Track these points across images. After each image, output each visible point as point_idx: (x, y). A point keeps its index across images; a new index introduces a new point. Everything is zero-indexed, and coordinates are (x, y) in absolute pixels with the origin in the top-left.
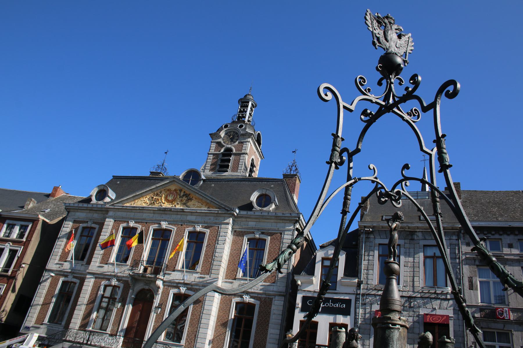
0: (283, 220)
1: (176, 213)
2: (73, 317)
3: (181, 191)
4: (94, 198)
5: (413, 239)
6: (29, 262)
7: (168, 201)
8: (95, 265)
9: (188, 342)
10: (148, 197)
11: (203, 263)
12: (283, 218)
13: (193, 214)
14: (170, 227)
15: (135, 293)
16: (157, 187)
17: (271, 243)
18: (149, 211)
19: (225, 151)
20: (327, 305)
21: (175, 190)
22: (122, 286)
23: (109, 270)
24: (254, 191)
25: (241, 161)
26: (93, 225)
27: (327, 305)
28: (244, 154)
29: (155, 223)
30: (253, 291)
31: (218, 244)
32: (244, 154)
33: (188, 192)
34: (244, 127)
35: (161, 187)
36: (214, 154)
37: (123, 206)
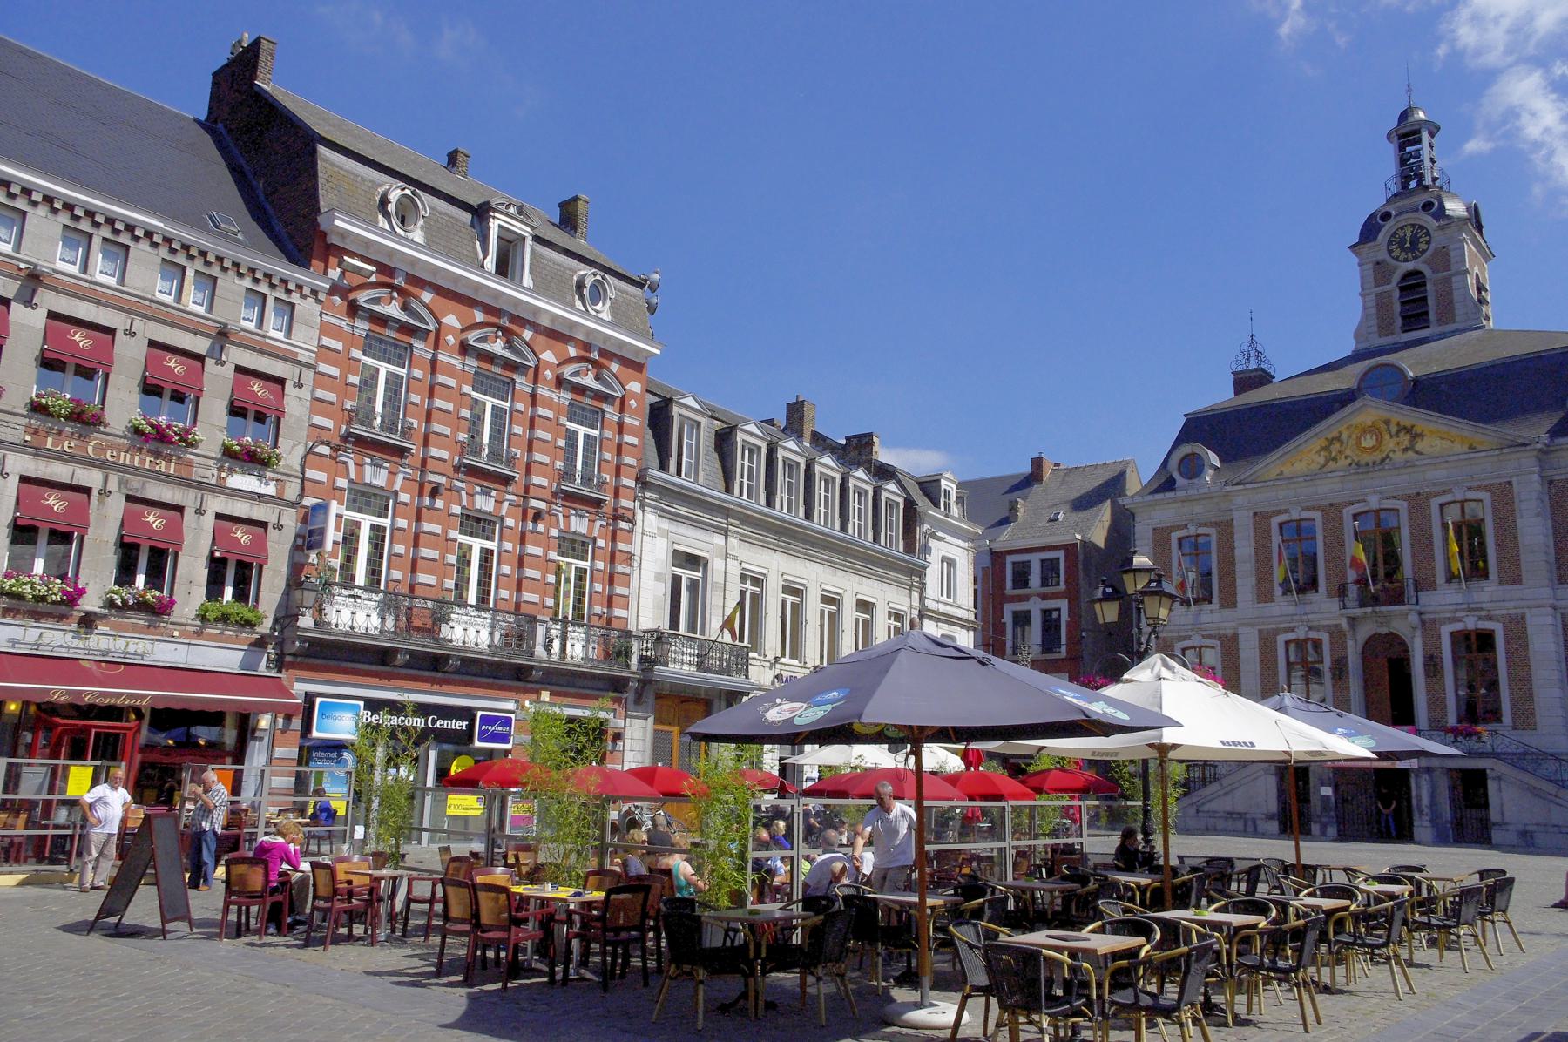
3: (1387, 422)
26: (1202, 530)
29: (1352, 503)
33: (1407, 422)
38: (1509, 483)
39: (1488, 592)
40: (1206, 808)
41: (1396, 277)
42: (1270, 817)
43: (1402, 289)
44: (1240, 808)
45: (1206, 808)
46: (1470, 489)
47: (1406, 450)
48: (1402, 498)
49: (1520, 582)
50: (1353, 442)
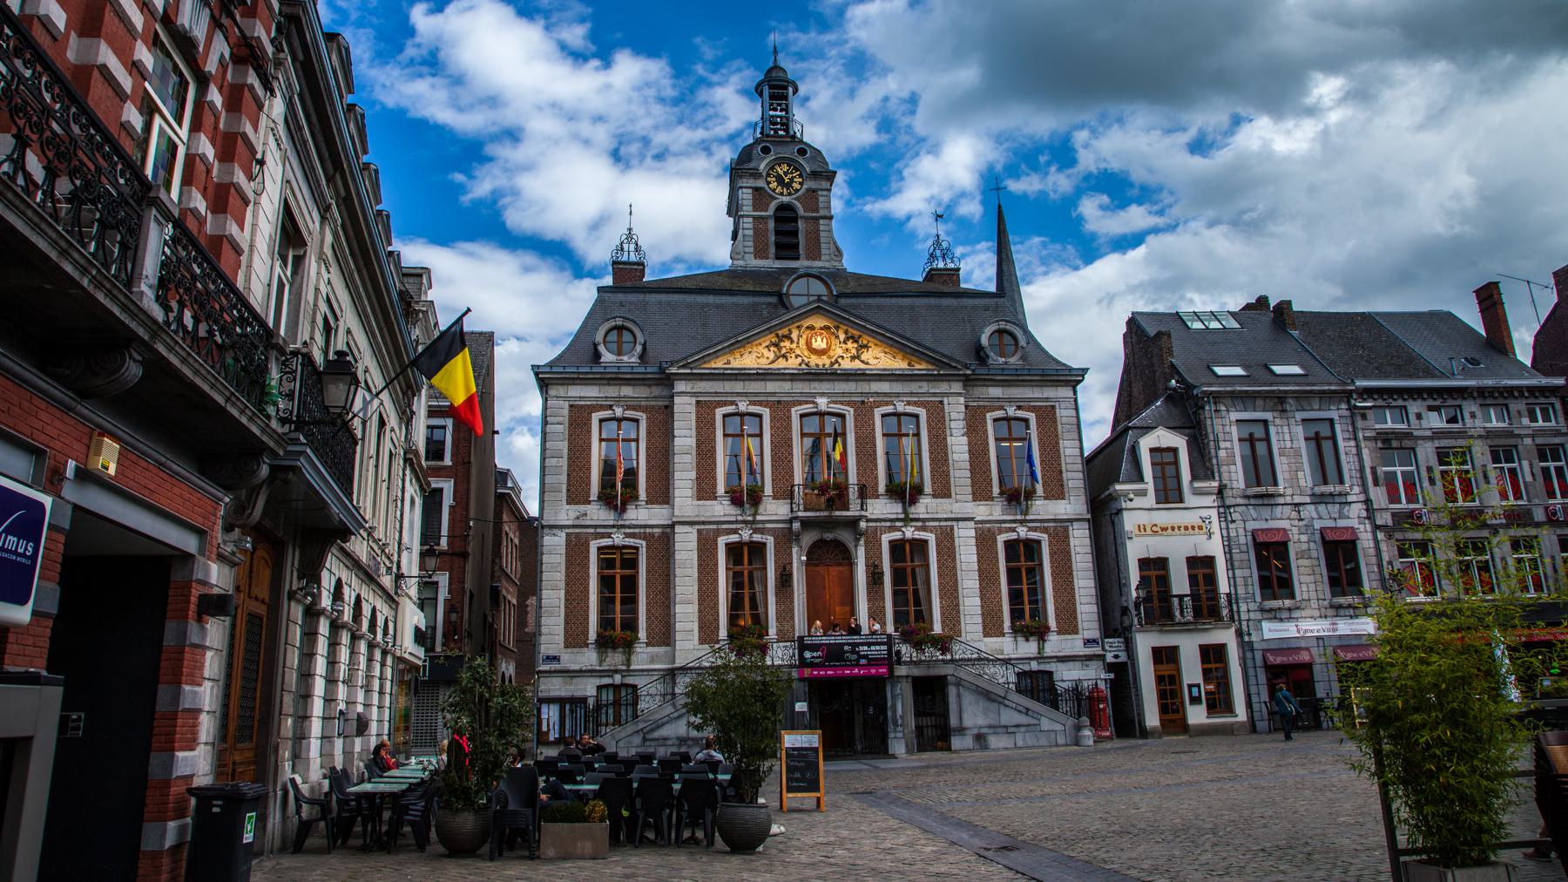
3: (837, 328)
5: (1284, 411)
11: (933, 476)
17: (1039, 426)
21: (826, 328)
22: (770, 541)
24: (985, 326)
29: (801, 403)
33: (856, 333)
36: (754, 218)
40: (656, 734)
41: (773, 205)
43: (777, 219)
45: (656, 734)
46: (909, 403)
47: (853, 358)
49: (949, 496)
50: (802, 342)
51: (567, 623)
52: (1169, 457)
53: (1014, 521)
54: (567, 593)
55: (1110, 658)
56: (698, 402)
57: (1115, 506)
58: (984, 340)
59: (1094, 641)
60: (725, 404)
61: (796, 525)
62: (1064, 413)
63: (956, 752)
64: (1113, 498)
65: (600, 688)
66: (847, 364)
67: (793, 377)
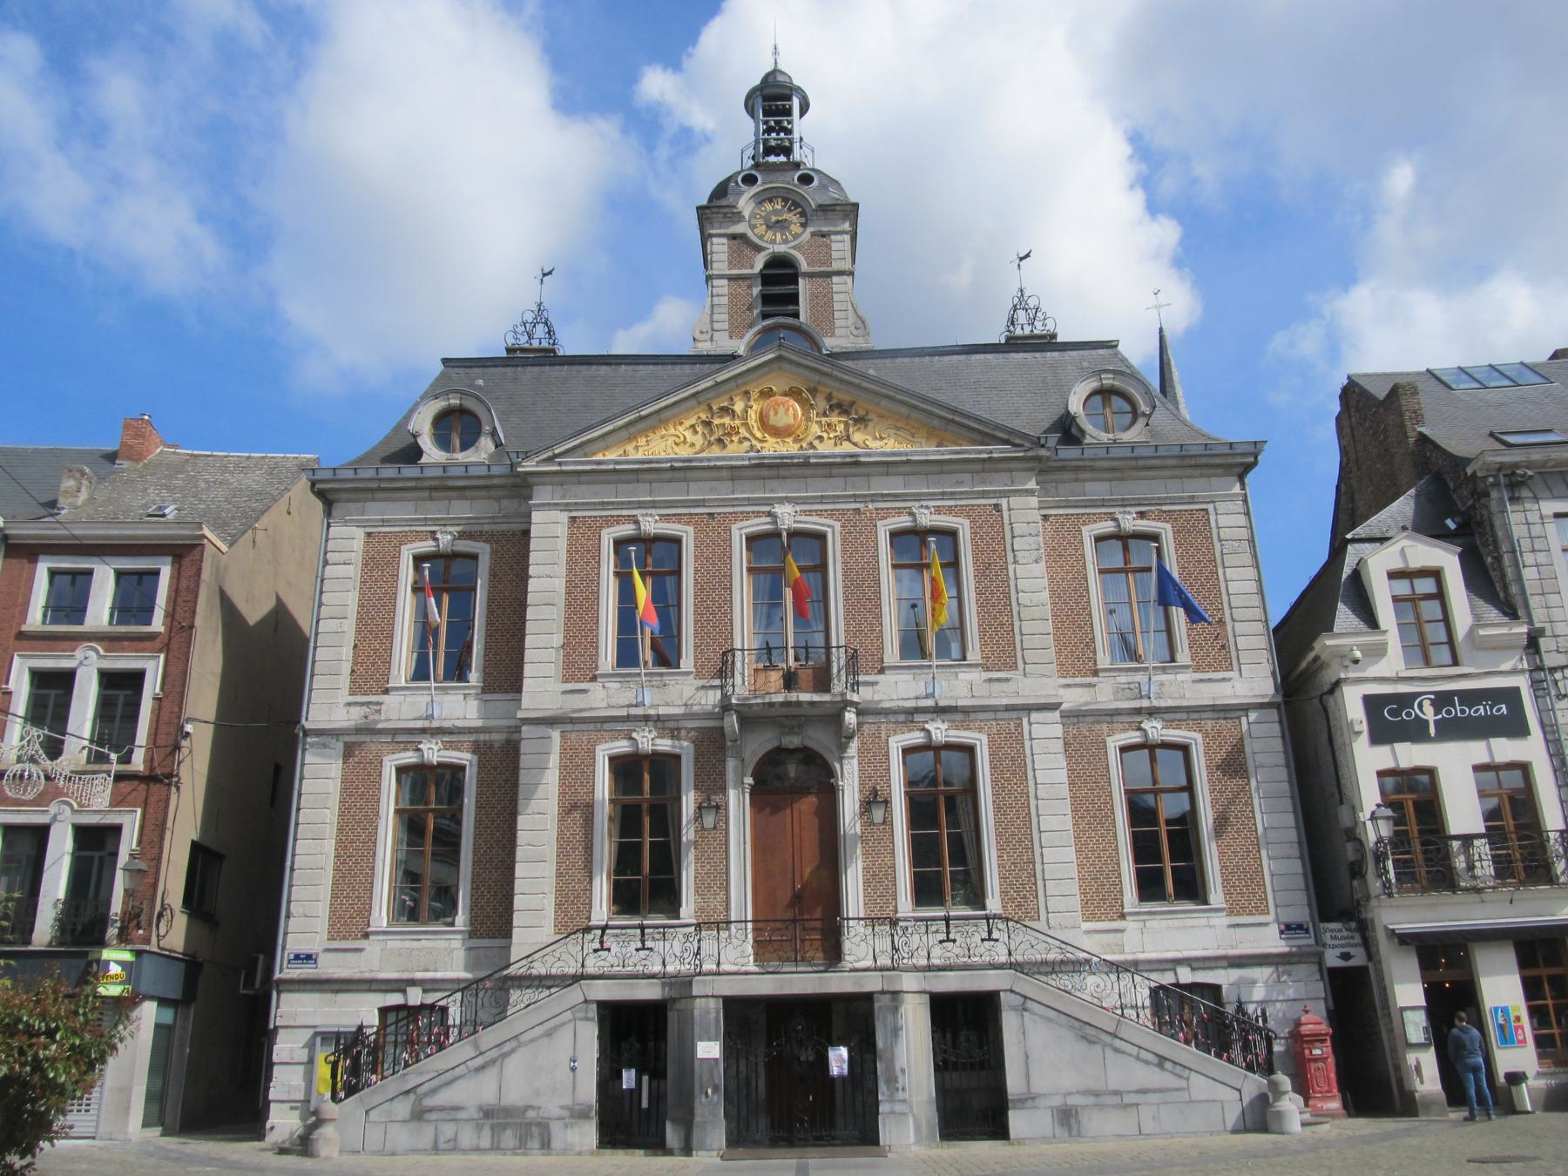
0: (1202, 466)
1: (825, 471)
2: (517, 889)
4: (426, 442)
6: (211, 714)
7: (778, 432)
8: (542, 687)
9: (1013, 900)
10: (687, 423)
11: (983, 633)
12: (1204, 461)
13: (892, 469)
14: (812, 523)
15: (750, 771)
16: (718, 384)
17: (1179, 545)
18: (714, 474)
19: (768, 265)
20: (1449, 712)
23: (613, 701)
25: (836, 297)
26: (465, 546)
27: (1449, 712)
28: (840, 273)
29: (747, 516)
30: (1170, 703)
31: (1015, 562)
32: (840, 273)
33: (843, 396)
34: (816, 182)
35: (732, 384)
36: (731, 278)
37: (599, 463)
38: (997, 507)
39: (962, 685)
40: (441, 1099)
42: (579, 1114)
44: (513, 1097)
46: (938, 510)
47: (838, 440)
48: (831, 514)
49: (1014, 667)
50: (753, 416)
51: (335, 896)
52: (1426, 586)
53: (1138, 711)
54: (339, 842)
55: (1332, 959)
56: (573, 519)
57: (1329, 676)
58: (1075, 405)
59: (1300, 927)
60: (618, 520)
61: (732, 721)
62: (1223, 520)
63: (1020, 1142)
64: (1318, 665)
65: (384, 1011)
66: (826, 448)
67: (734, 473)
